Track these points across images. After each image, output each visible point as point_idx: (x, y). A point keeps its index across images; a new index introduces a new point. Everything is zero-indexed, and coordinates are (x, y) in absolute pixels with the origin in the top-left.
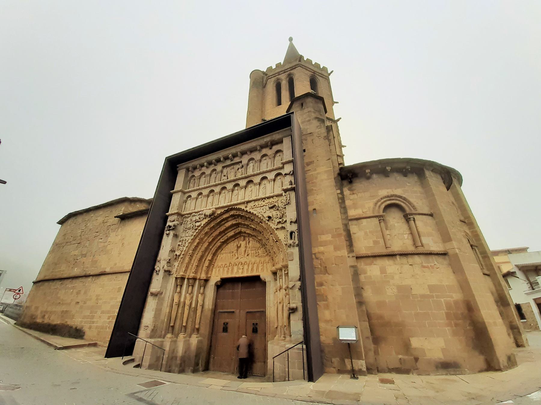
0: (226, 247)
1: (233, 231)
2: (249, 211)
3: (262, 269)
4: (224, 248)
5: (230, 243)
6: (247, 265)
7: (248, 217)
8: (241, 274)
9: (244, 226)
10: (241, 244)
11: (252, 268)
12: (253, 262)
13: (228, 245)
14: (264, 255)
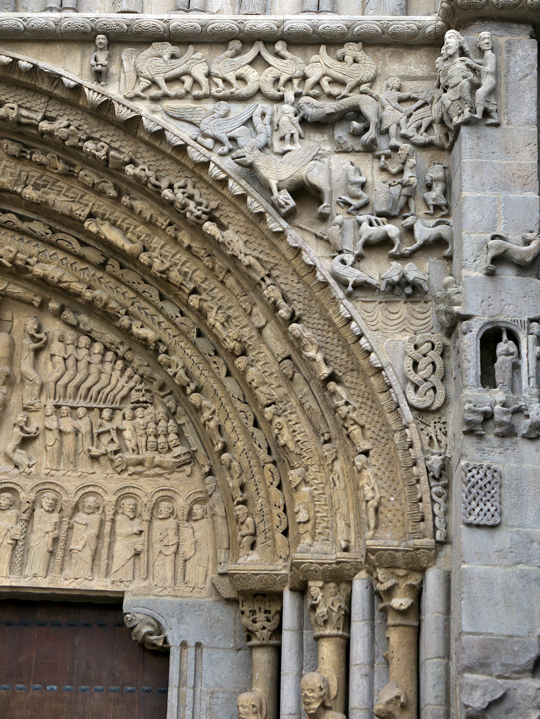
2: (123, 114)
3: (137, 554)
6: (12, 513)
7: (101, 154)
9: (21, 218)
14: (158, 458)
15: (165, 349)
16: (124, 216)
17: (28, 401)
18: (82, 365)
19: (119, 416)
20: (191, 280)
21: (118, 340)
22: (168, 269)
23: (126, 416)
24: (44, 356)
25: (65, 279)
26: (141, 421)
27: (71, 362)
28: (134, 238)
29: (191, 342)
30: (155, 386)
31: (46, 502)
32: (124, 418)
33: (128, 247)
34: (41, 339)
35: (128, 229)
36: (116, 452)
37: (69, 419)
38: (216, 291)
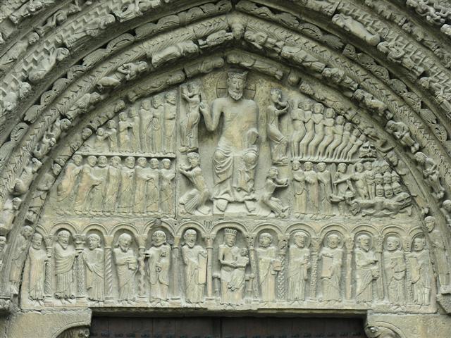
0: (123, 125)
1: (190, 31)
3: (374, 280)
4: (105, 125)
5: (146, 102)
6: (273, 248)
8: (237, 295)
9: (274, 11)
10: (222, 115)
11: (309, 270)
12: (316, 237)
13: (134, 110)
14: (387, 202)
15: (391, 116)
16: (365, 13)
17: (277, 158)
18: (319, 128)
19: (352, 167)
20: (421, 65)
21: (348, 107)
22: (402, 57)
23: (358, 169)
24: (286, 120)
25: (310, 58)
26: (371, 173)
27: (309, 126)
28: (373, 31)
29: (415, 112)
30: (378, 144)
31: (298, 241)
32: (356, 170)
33: (369, 38)
34: (285, 107)
35: (368, 23)
36: (352, 198)
37: (313, 172)
38: (443, 74)
